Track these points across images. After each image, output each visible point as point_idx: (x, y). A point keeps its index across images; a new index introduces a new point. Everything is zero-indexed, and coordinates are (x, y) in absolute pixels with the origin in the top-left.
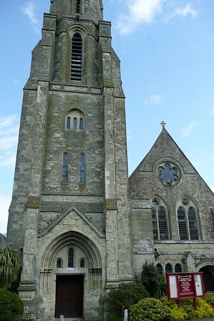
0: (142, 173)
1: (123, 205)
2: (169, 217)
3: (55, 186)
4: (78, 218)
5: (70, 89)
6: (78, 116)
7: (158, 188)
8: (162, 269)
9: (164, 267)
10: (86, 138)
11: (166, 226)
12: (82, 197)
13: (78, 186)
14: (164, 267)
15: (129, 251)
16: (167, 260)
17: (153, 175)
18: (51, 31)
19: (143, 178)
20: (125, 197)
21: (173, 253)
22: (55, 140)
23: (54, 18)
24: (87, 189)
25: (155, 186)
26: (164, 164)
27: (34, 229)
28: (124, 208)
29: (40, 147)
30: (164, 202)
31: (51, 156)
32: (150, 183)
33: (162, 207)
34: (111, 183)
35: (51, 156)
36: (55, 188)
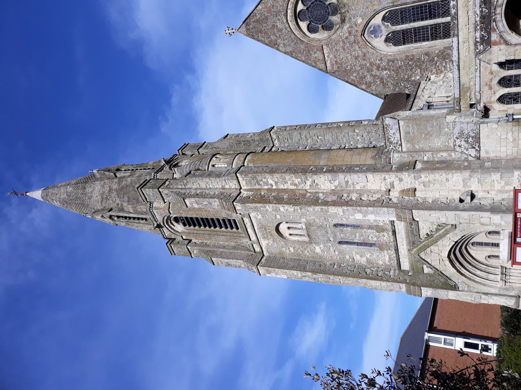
0: (328, 65)
1: (401, 180)
2: (405, 4)
3: (387, 256)
4: (428, 250)
5: (251, 230)
6: (283, 228)
7: (350, 33)
8: (509, 94)
9: (506, 91)
10: (311, 222)
11: (417, 8)
12: (396, 230)
13: (382, 233)
14: (506, 91)
15: (475, 176)
16: (491, 88)
17: (327, 45)
18: (190, 250)
19: (336, 62)
20: (387, 177)
21: (478, 74)
22: (326, 253)
23: (171, 246)
24: (385, 224)
25: (346, 38)
26: (300, 23)
27: (448, 292)
28: (405, 180)
29: (341, 279)
30: (373, 17)
31: (347, 257)
32: (344, 49)
33: (384, 19)
34: (372, 213)
35: (347, 257)
36: (389, 256)
